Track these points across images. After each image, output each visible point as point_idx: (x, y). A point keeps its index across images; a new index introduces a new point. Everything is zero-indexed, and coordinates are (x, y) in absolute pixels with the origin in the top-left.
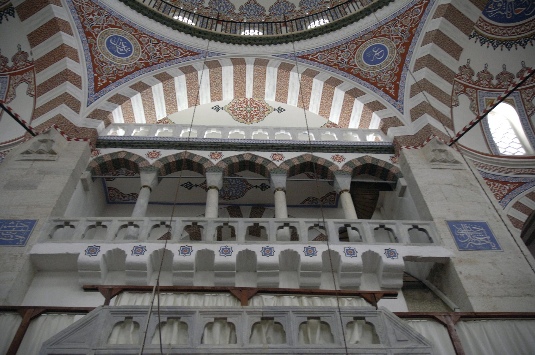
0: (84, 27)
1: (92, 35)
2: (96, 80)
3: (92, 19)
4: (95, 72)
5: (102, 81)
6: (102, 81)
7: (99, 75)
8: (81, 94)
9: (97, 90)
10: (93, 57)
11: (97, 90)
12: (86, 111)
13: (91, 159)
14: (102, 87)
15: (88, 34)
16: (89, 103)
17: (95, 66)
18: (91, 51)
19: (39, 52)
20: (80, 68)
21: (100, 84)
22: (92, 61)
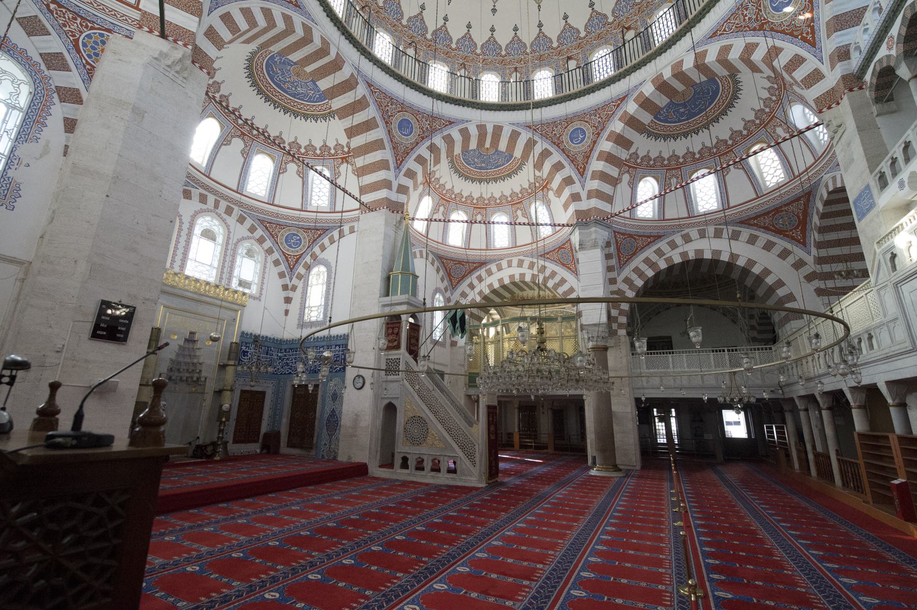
0: (754, 29)
1: (763, 24)
2: (804, 40)
3: (749, 19)
4: (796, 37)
5: (807, 34)
6: (807, 34)
7: (801, 34)
8: (811, 64)
9: (813, 45)
10: (783, 32)
11: (813, 45)
12: (825, 69)
13: (868, 93)
14: (813, 37)
15: (761, 28)
16: (821, 60)
17: (791, 34)
18: (777, 31)
19: (768, 72)
20: (790, 49)
21: (809, 37)
22: (786, 34)
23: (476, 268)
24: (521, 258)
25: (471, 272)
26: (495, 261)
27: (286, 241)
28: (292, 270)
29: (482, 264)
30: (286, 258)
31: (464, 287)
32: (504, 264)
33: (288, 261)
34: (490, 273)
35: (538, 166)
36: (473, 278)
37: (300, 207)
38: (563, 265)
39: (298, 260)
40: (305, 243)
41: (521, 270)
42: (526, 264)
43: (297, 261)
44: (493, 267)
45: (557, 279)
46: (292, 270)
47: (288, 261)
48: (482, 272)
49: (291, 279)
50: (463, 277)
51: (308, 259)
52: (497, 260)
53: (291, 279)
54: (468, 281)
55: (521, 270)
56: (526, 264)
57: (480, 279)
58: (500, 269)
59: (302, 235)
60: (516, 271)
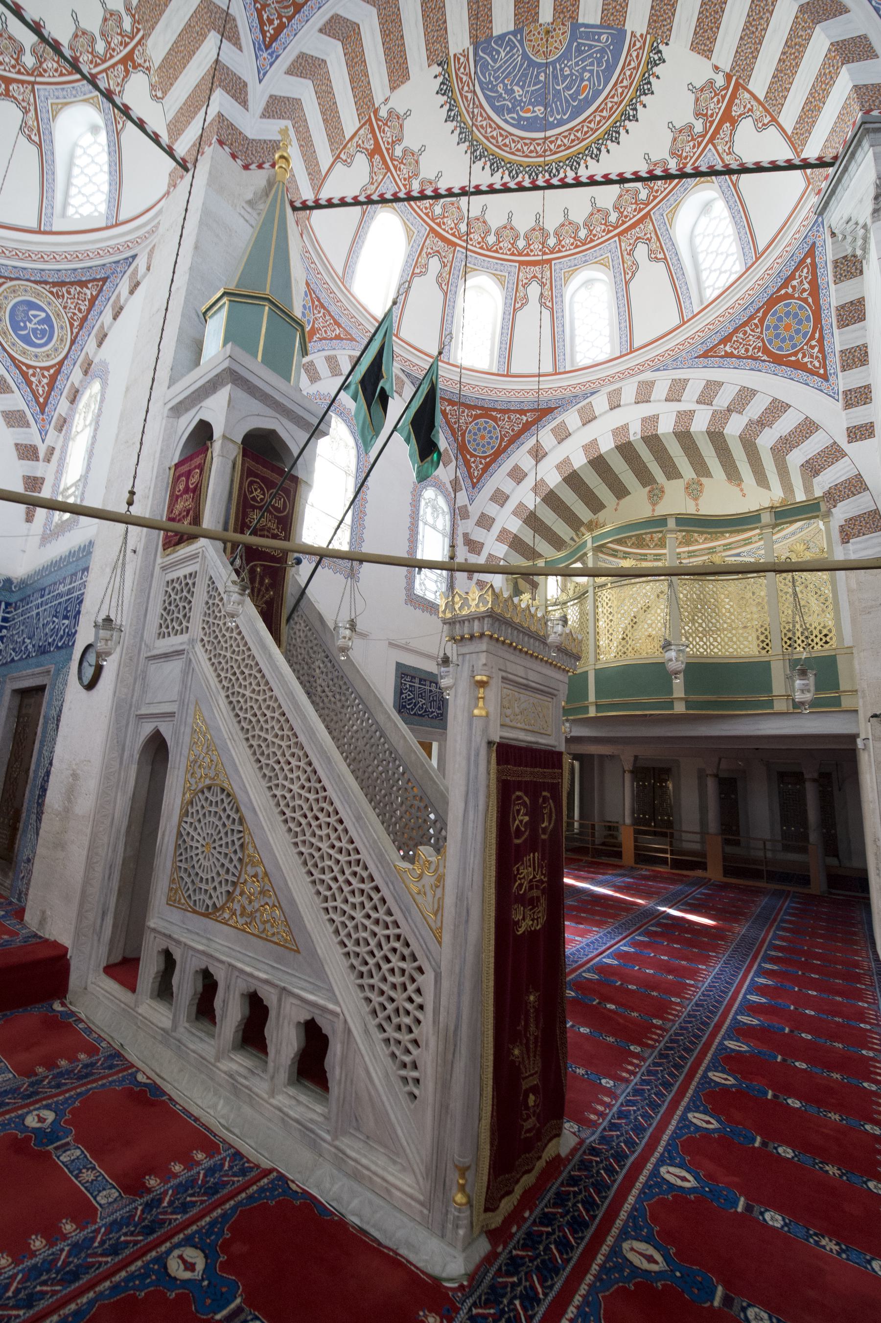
23: (527, 427)
24: (648, 376)
25: (515, 438)
26: (573, 400)
27: (16, 327)
28: (42, 407)
29: (543, 413)
30: (24, 375)
31: (499, 479)
32: (600, 402)
33: (29, 384)
34: (562, 435)
35: (704, 41)
36: (521, 456)
37: (34, 225)
38: (778, 360)
39: (53, 379)
40: (62, 330)
41: (646, 410)
42: (661, 390)
43: (52, 385)
44: (571, 418)
45: (755, 409)
46: (42, 407)
47: (29, 384)
48: (545, 436)
49: (43, 433)
50: (499, 453)
51: (76, 375)
52: (577, 398)
53: (43, 433)
54: (507, 466)
55: (646, 410)
56: (661, 390)
57: (538, 454)
58: (588, 418)
59: (51, 305)
60: (632, 418)
